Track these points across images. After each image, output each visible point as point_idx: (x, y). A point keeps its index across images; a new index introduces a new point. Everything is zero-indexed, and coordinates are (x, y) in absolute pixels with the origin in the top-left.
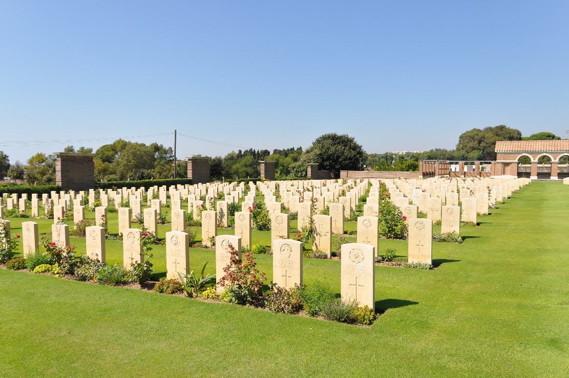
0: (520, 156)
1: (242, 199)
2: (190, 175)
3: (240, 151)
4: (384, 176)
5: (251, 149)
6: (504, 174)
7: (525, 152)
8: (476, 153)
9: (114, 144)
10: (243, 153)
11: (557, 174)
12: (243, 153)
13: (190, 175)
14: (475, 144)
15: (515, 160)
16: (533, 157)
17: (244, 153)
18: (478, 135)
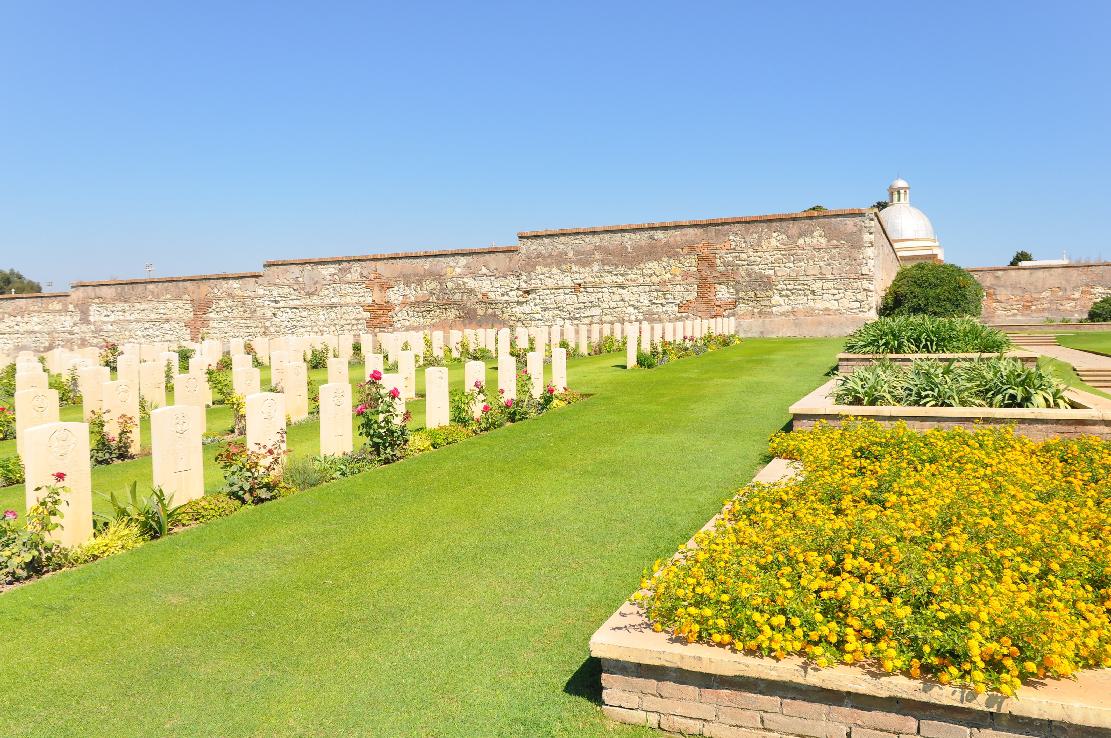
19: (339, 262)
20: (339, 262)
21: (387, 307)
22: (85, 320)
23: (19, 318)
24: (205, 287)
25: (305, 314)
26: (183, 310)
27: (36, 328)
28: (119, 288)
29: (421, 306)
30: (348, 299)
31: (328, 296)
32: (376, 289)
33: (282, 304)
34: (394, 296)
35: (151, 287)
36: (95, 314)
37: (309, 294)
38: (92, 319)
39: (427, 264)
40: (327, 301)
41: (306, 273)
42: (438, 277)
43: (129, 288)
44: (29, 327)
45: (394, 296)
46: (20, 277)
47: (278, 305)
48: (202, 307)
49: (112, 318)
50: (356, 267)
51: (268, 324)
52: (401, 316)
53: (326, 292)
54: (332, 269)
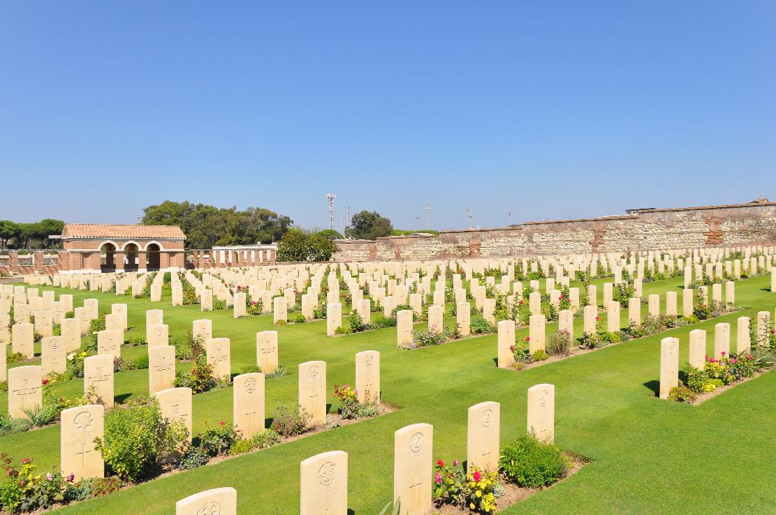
1: (433, 288)
6: (169, 266)
11: (145, 266)
19: (689, 210)
20: (689, 210)
21: (722, 233)
22: (530, 240)
23: (493, 240)
24: (602, 225)
25: (665, 237)
26: (590, 236)
27: (503, 245)
28: (551, 225)
29: (744, 232)
30: (694, 230)
31: (678, 228)
32: (712, 224)
33: (650, 232)
34: (724, 227)
35: (570, 224)
36: (537, 238)
37: (668, 227)
38: (534, 240)
39: (747, 211)
40: (679, 230)
41: (666, 216)
42: (756, 218)
43: (556, 226)
44: (498, 244)
45: (724, 227)
46: (378, 216)
47: (647, 233)
48: (599, 235)
49: (546, 240)
50: (699, 214)
51: (640, 242)
52: (728, 239)
53: (679, 226)
54: (683, 214)
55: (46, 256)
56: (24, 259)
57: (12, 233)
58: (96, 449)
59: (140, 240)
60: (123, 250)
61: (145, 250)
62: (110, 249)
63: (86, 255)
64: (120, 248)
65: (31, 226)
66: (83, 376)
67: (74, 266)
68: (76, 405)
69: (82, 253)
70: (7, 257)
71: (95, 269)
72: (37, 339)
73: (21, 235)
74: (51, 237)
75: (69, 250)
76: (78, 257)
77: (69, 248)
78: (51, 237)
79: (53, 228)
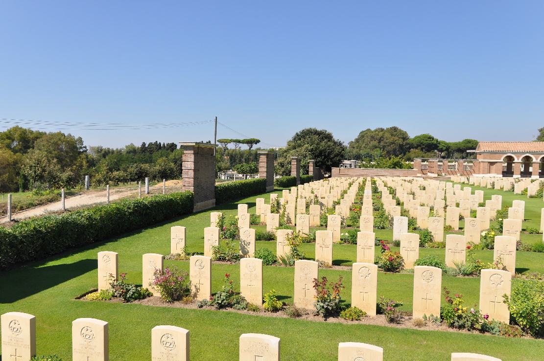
0: (506, 155)
2: (311, 174)
3: (144, 144)
4: (383, 173)
5: (157, 141)
7: (512, 153)
8: (377, 152)
9: (10, 131)
10: (147, 146)
12: (147, 146)
13: (311, 174)
14: (375, 143)
15: (500, 159)
16: (516, 156)
17: (149, 145)
18: (378, 135)
55: (464, 164)
56: (451, 166)
57: (444, 148)
58: (504, 302)
59: (534, 153)
60: (520, 161)
61: (539, 161)
62: (510, 160)
63: (492, 164)
64: (518, 160)
65: (456, 144)
66: (492, 248)
67: (483, 171)
68: (488, 268)
69: (489, 162)
70: (441, 163)
71: (498, 174)
72: (461, 218)
73: (450, 150)
74: (468, 151)
75: (480, 160)
76: (486, 165)
77: (480, 159)
78: (468, 151)
79: (470, 145)
